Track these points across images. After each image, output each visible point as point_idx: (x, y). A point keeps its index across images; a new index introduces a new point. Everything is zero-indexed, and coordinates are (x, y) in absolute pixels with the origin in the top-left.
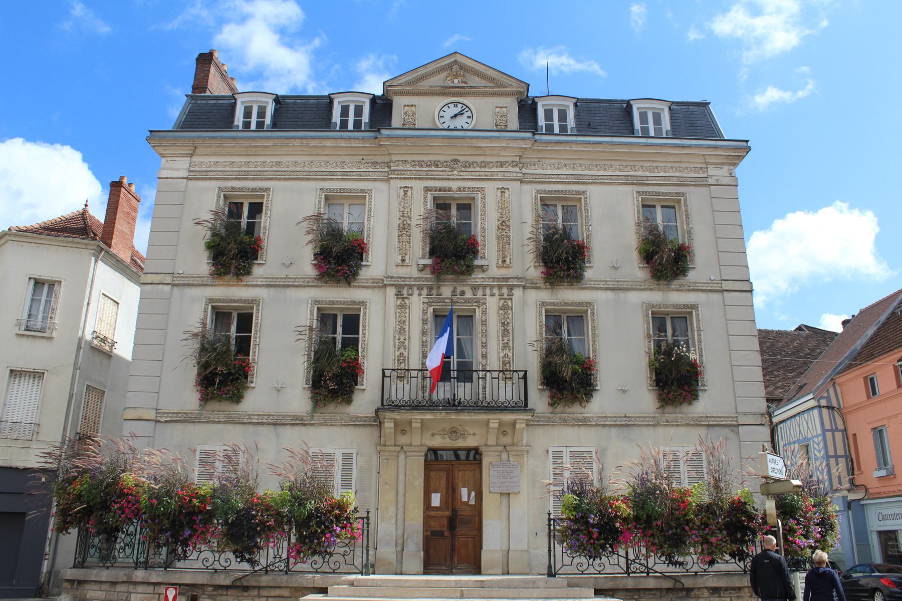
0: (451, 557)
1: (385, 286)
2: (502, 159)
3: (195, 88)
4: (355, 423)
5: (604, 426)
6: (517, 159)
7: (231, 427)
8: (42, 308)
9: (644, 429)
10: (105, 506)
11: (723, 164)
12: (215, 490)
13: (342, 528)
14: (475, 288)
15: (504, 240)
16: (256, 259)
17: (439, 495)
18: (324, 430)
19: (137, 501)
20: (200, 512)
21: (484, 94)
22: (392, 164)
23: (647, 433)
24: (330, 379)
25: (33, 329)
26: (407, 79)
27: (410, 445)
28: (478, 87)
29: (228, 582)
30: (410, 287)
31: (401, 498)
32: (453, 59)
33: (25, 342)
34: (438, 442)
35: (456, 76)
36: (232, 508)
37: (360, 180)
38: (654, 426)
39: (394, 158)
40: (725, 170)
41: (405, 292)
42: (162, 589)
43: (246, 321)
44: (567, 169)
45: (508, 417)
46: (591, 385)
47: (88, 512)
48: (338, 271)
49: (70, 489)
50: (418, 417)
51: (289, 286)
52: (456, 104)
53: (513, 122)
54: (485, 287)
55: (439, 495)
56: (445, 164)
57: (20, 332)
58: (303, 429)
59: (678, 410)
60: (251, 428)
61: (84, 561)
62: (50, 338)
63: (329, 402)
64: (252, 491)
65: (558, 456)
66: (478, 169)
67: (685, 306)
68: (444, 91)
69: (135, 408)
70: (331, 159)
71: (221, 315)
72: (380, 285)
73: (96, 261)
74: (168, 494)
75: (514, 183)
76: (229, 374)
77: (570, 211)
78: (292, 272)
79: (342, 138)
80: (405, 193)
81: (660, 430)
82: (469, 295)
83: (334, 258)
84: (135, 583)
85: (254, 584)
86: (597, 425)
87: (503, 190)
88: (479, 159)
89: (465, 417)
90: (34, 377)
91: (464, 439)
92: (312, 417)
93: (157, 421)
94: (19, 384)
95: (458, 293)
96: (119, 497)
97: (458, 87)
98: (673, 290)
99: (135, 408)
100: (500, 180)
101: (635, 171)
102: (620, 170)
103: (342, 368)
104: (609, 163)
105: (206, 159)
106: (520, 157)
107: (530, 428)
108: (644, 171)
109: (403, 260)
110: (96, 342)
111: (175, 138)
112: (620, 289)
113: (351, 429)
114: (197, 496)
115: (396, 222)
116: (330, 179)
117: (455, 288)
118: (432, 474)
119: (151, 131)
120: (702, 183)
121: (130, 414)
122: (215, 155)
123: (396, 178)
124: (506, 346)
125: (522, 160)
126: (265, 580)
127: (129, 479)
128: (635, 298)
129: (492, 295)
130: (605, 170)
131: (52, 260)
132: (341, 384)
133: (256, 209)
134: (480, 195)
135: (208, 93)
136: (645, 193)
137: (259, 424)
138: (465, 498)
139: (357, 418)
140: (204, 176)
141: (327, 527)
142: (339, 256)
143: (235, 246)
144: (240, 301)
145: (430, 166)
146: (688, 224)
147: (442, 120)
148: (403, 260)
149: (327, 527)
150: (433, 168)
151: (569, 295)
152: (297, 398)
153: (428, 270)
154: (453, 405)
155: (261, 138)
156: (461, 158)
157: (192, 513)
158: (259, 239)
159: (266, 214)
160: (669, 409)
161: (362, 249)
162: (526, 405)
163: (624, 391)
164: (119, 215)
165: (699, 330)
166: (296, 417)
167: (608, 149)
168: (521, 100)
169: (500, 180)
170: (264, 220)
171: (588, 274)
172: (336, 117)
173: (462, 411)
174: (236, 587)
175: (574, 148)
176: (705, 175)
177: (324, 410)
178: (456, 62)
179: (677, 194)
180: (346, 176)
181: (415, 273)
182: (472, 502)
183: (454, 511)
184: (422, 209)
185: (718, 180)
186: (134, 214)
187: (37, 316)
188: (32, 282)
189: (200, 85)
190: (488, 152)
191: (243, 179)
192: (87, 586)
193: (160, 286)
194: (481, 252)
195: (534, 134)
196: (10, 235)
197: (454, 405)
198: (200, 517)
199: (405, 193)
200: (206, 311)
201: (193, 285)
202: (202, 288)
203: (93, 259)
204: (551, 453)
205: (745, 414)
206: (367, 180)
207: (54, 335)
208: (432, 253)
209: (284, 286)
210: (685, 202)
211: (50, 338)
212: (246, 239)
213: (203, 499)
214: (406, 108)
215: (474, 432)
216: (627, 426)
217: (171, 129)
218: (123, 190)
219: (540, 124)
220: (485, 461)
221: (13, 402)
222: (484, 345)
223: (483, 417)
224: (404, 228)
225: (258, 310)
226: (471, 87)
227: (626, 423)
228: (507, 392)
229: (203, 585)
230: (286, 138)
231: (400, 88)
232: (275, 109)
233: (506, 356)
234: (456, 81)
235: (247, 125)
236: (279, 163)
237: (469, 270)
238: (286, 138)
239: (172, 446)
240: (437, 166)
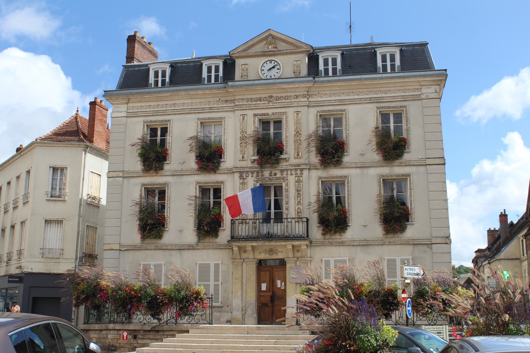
0: (272, 317)
1: (234, 172)
2: (297, 94)
3: (127, 58)
4: (220, 247)
5: (353, 245)
6: (306, 93)
7: (157, 252)
8: (58, 184)
9: (376, 247)
10: (94, 295)
11: (432, 85)
12: (141, 287)
13: (199, 303)
14: (282, 171)
15: (298, 143)
16: (165, 160)
17: (265, 284)
18: (204, 252)
19: (107, 293)
20: (135, 297)
21: (287, 54)
22: (235, 102)
23: (378, 249)
24: (206, 225)
25: (56, 195)
26: (242, 48)
27: (248, 258)
28: (283, 50)
29: (149, 329)
30: (247, 172)
31: (244, 286)
32: (268, 33)
33: (52, 204)
34: (263, 256)
35: (270, 44)
36: (149, 295)
37: (219, 112)
38: (382, 245)
39: (237, 98)
40: (433, 89)
41: (244, 175)
42: (121, 332)
43: (162, 194)
44: (335, 97)
45: (296, 243)
46: (346, 222)
47: (87, 299)
48: (208, 166)
49: (79, 288)
50: (249, 245)
51: (183, 175)
52: (271, 61)
53: (304, 71)
54: (287, 170)
55: (265, 284)
56: (265, 99)
57: (48, 199)
58: (194, 251)
59: (395, 236)
60: (167, 252)
61: (88, 320)
62: (64, 201)
63: (206, 237)
64: (158, 287)
65: (327, 263)
66: (284, 101)
67: (403, 175)
68: (264, 54)
69: (109, 244)
70: (203, 100)
71: (149, 191)
72: (230, 171)
73: (85, 153)
74: (120, 289)
75: (304, 107)
76: (154, 224)
77: (339, 121)
78: (185, 167)
79: (207, 89)
80: (244, 118)
81: (385, 247)
82: (279, 175)
83: (205, 159)
84: (110, 330)
85: (161, 329)
86: (349, 245)
87: (298, 112)
88: (284, 95)
89: (273, 243)
90: (58, 223)
91: (277, 254)
92: (198, 245)
93: (120, 250)
94: (50, 227)
95: (273, 174)
96: (100, 291)
97: (271, 51)
98: (396, 166)
99: (109, 244)
100: (296, 106)
101: (376, 94)
102: (367, 94)
103: (212, 219)
104: (360, 91)
105: (136, 105)
106: (308, 91)
107: (312, 247)
108: (382, 94)
109: (243, 157)
110: (89, 200)
111: (117, 95)
112: (364, 167)
113: (218, 250)
114: (133, 290)
115: (239, 135)
116: (203, 112)
117: (271, 172)
118: (262, 273)
119: (105, 91)
120: (417, 98)
121: (107, 247)
122: (140, 102)
123: (238, 110)
124: (299, 203)
125: (309, 93)
126: (166, 327)
127: (103, 283)
128: (374, 172)
129: (292, 174)
130: (358, 95)
131: (61, 155)
132: (211, 227)
133: (164, 131)
134: (284, 117)
135: (136, 63)
136: (382, 108)
137: (171, 249)
138: (279, 286)
139: (221, 245)
140: (135, 115)
141: (191, 303)
142: (209, 156)
143: (154, 154)
144: (158, 184)
145: (256, 101)
146: (407, 125)
147: (263, 72)
148: (243, 157)
149: (191, 303)
150: (259, 102)
151: (335, 172)
152: (190, 235)
153: (256, 163)
154: (269, 237)
155: (163, 92)
156: (274, 95)
157: (131, 298)
158: (167, 150)
159: (169, 135)
160: (390, 235)
161: (221, 152)
162: (308, 236)
163: (365, 226)
164: (97, 122)
165: (411, 189)
166: (190, 245)
167: (358, 83)
168: (310, 54)
169: (296, 106)
170: (168, 138)
171: (346, 159)
172: (205, 74)
173: (272, 240)
174: (153, 331)
175: (338, 84)
176: (419, 93)
177: (203, 241)
178: (270, 35)
179: (401, 107)
180: (211, 110)
181: (249, 164)
182: (283, 288)
183: (273, 292)
184: (253, 127)
185: (427, 96)
186: (105, 119)
187: (56, 188)
188: (52, 169)
189: (130, 57)
190: (289, 90)
191: (156, 115)
192: (90, 332)
193: (117, 178)
194: (285, 150)
195: (314, 78)
196: (37, 143)
197: (268, 238)
198: (135, 299)
199: (244, 118)
200: (141, 191)
201: (134, 177)
202: (139, 178)
203: (84, 152)
204: (324, 261)
205: (436, 237)
206: (223, 111)
207: (66, 198)
208: (258, 153)
209: (181, 175)
210: (406, 111)
211: (64, 201)
212: (159, 150)
213: (136, 291)
214: (243, 66)
215: (283, 250)
216: (367, 245)
217: (115, 89)
218: (97, 106)
219: (320, 69)
220: (288, 266)
221: (48, 238)
222: (287, 203)
223: (283, 243)
224: (243, 138)
225: (168, 189)
226: (279, 51)
227: (365, 244)
228: (299, 229)
229: (139, 330)
230: (177, 91)
231: (238, 55)
232: (171, 71)
233: (299, 208)
234: (270, 47)
235: (156, 82)
236: (174, 105)
237: (277, 161)
238: (177, 91)
239: (124, 265)
240: (261, 101)
